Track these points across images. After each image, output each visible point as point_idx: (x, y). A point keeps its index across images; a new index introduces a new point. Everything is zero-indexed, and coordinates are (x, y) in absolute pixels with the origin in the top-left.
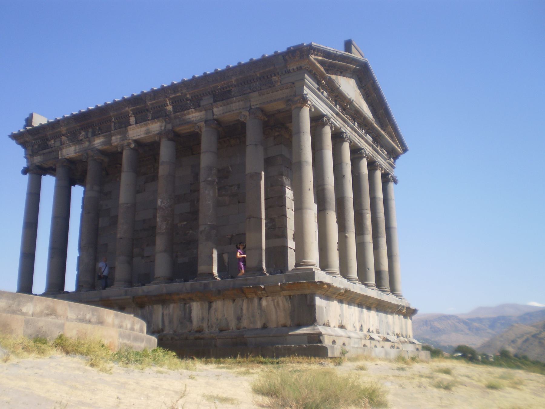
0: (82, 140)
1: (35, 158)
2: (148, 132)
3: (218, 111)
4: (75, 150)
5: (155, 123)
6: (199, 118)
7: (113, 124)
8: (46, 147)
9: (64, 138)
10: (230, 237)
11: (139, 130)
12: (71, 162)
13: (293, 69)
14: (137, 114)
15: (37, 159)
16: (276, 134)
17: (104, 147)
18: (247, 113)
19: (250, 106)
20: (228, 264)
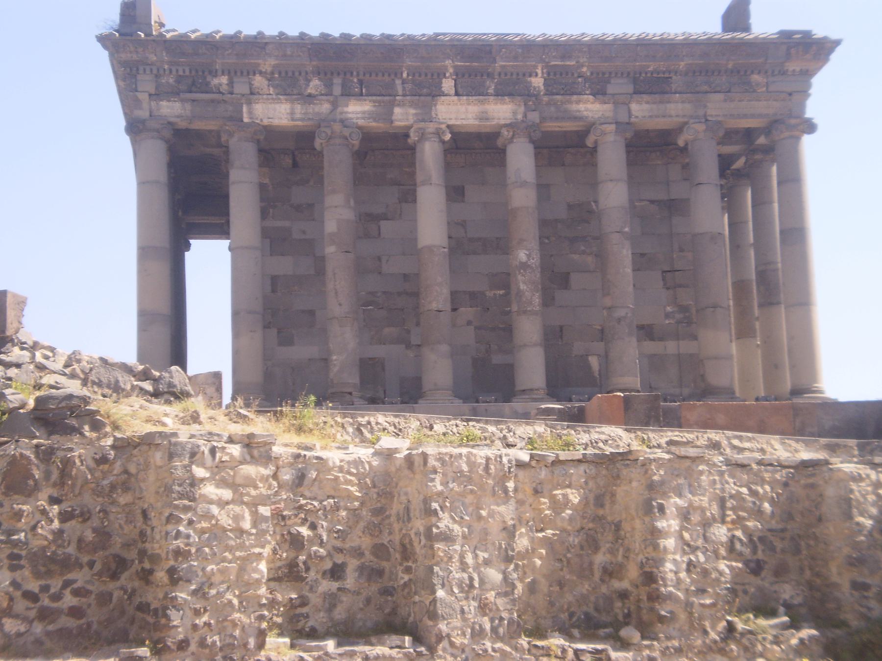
0: (310, 95)
1: (164, 103)
3: (641, 110)
4: (292, 113)
7: (398, 82)
8: (206, 88)
9: (259, 81)
10: (600, 328)
11: (463, 109)
12: (270, 132)
13: (794, 71)
15: (171, 109)
17: (374, 124)
18: (701, 127)
19: (705, 115)
20: (600, 375)
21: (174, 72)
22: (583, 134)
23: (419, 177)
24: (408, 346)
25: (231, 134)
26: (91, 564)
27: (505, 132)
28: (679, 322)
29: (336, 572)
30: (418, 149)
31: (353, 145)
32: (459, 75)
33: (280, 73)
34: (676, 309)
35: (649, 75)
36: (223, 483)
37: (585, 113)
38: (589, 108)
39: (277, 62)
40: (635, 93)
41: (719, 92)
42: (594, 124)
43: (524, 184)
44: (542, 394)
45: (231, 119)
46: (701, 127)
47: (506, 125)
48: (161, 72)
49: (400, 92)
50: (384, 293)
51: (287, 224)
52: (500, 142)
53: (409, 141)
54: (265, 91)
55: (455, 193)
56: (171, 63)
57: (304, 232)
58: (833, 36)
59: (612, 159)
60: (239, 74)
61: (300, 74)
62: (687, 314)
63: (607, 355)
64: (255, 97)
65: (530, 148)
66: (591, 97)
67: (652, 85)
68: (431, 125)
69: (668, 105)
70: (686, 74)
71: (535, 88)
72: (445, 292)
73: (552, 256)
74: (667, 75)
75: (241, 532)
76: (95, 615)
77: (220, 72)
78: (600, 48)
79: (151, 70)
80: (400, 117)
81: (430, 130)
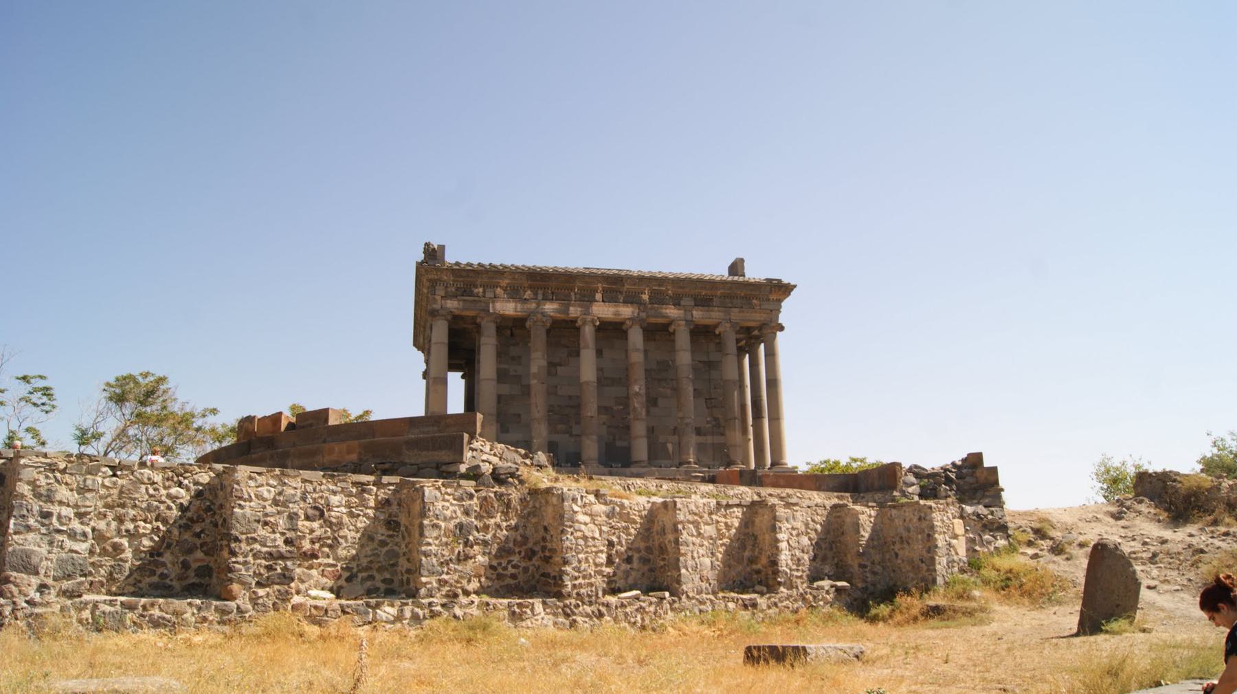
2: (617, 314)
3: (698, 315)
8: (471, 294)
12: (504, 318)
15: (452, 304)
22: (669, 324)
23: (582, 345)
24: (571, 435)
26: (520, 553)
29: (629, 560)
36: (586, 514)
38: (672, 312)
43: (638, 350)
51: (506, 366)
52: (624, 327)
55: (599, 353)
59: (683, 338)
75: (594, 538)
76: (521, 578)
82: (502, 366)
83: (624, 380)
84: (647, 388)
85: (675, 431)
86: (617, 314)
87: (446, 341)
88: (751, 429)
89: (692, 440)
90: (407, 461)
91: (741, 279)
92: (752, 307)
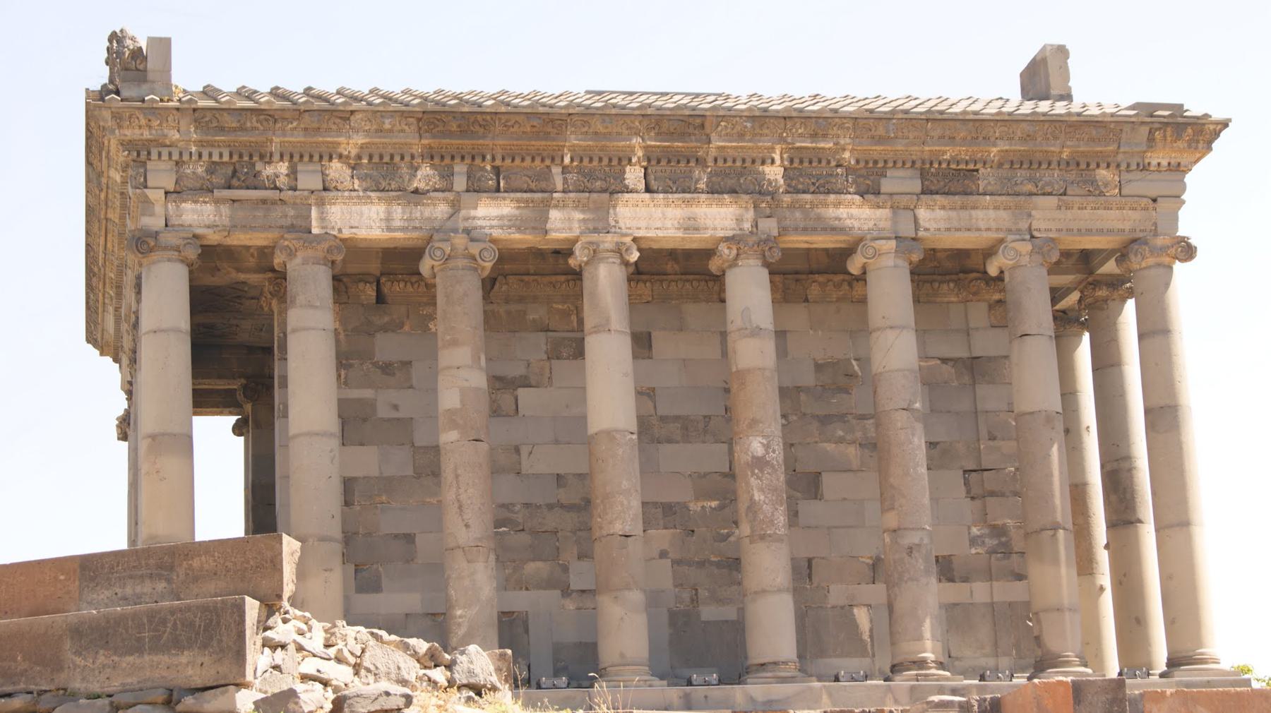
0: (416, 191)
1: (188, 206)
2: (690, 225)
4: (388, 219)
5: (721, 204)
6: (871, 224)
7: (556, 170)
9: (337, 170)
10: (870, 562)
11: (658, 213)
12: (353, 249)
14: (659, 162)
15: (199, 215)
16: (997, 297)
17: (517, 236)
20: (871, 636)
21: (205, 157)
24: (566, 592)
25: (292, 254)
27: (724, 249)
28: (992, 552)
30: (586, 275)
31: (483, 268)
32: (651, 159)
33: (371, 157)
34: (986, 531)
35: (944, 166)
37: (848, 223)
38: (854, 214)
39: (367, 140)
40: (923, 193)
41: (1050, 194)
42: (861, 240)
43: (756, 332)
44: (791, 671)
45: (293, 226)
46: (1026, 247)
47: (726, 239)
48: (186, 157)
49: (560, 186)
50: (527, 505)
51: (367, 393)
52: (714, 266)
53: (571, 262)
54: (348, 184)
55: (642, 343)
56: (200, 143)
57: (396, 407)
58: (1217, 115)
59: (890, 292)
60: (306, 159)
61: (402, 158)
62: (1003, 539)
63: (891, 608)
64: (331, 194)
65: (764, 273)
66: (857, 197)
67: (950, 181)
68: (609, 237)
69: (973, 212)
70: (1000, 165)
71: (770, 182)
72: (636, 504)
73: (792, 445)
74: (971, 166)
77: (276, 157)
78: (873, 124)
79: (170, 154)
80: (559, 225)
81: (608, 246)
82: (355, 394)
83: (717, 423)
84: (789, 446)
85: (876, 570)
86: (690, 225)
87: (184, 323)
88: (1103, 558)
89: (928, 595)
90: (77, 685)
91: (1060, 108)
92: (1095, 191)
